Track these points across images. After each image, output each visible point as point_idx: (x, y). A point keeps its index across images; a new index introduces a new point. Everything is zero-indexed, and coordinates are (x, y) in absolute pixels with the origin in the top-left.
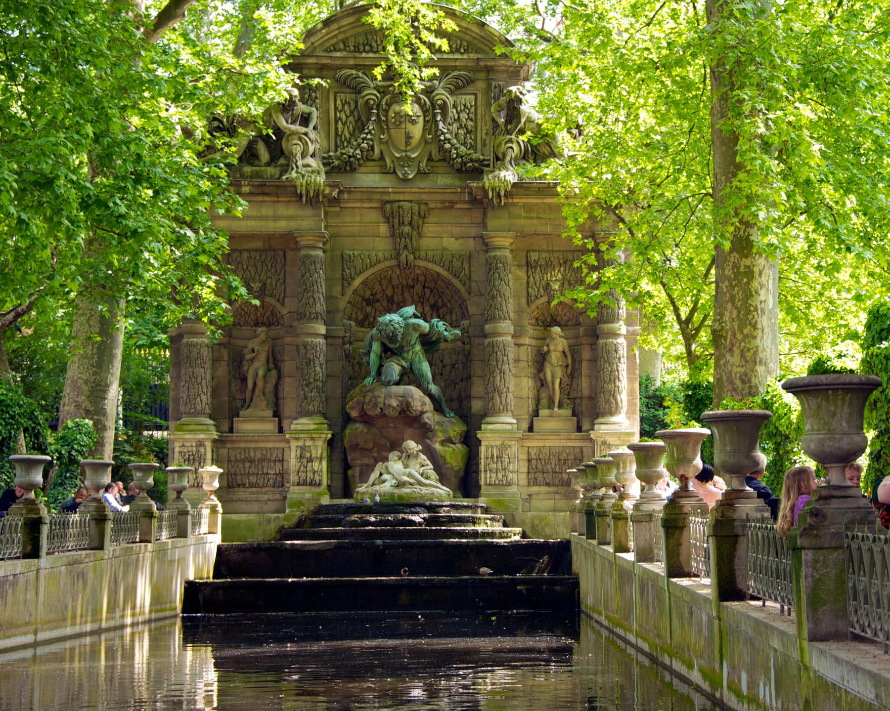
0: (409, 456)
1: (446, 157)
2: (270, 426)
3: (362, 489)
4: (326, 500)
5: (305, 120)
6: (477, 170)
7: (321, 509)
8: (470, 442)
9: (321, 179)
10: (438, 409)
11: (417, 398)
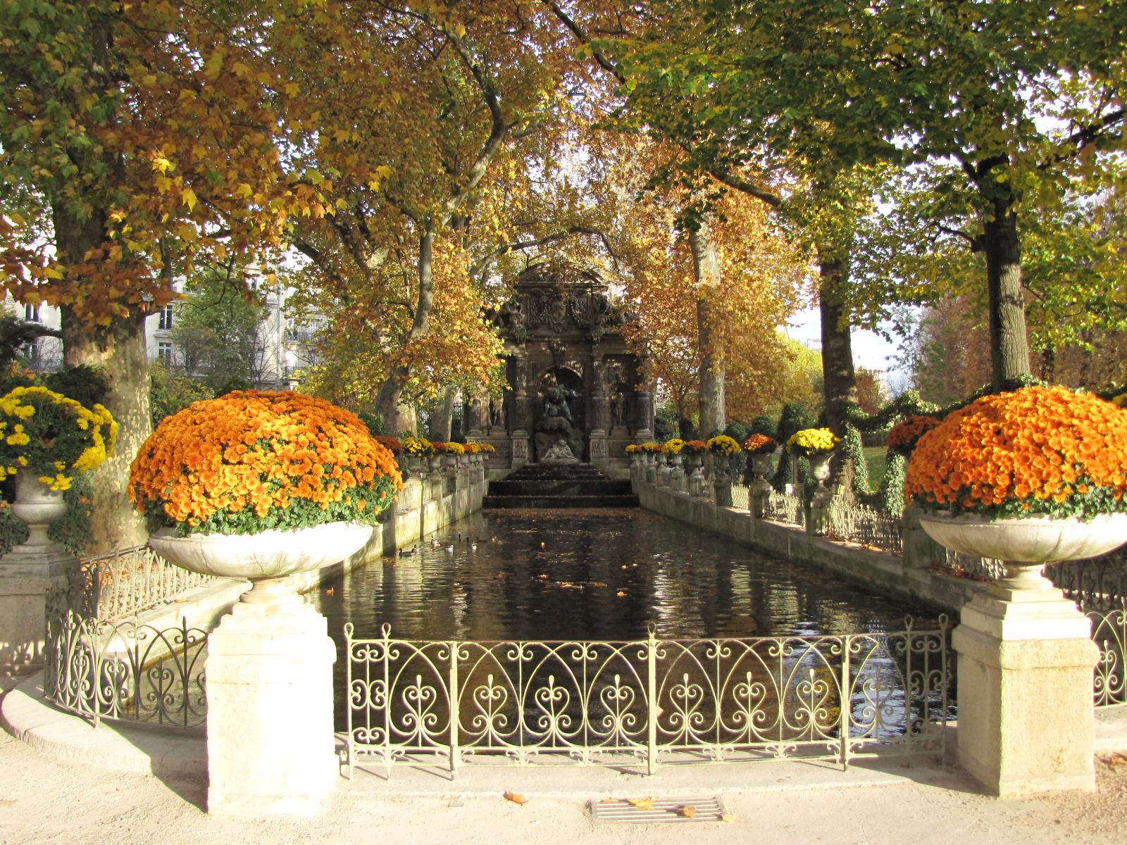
0: (560, 446)
1: (575, 323)
2: (504, 434)
3: (543, 459)
4: (528, 464)
5: (518, 308)
6: (587, 329)
7: (525, 467)
8: (586, 440)
9: (525, 333)
10: (572, 426)
11: (566, 424)
